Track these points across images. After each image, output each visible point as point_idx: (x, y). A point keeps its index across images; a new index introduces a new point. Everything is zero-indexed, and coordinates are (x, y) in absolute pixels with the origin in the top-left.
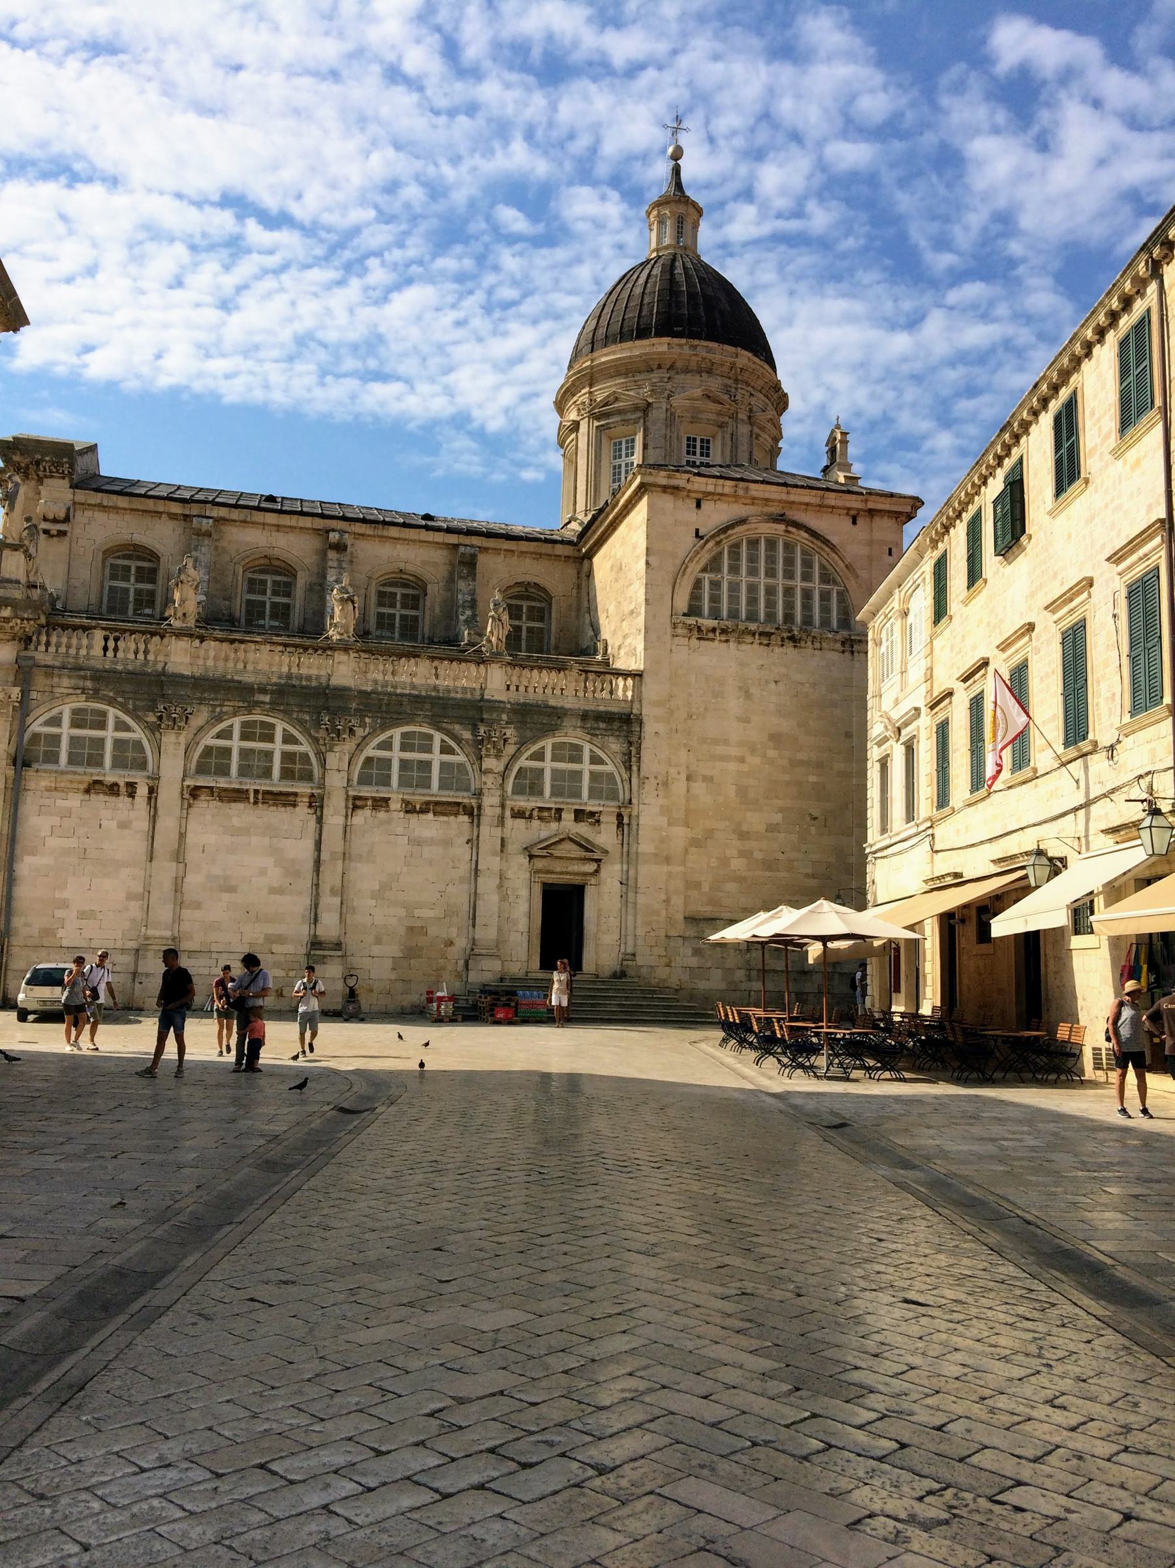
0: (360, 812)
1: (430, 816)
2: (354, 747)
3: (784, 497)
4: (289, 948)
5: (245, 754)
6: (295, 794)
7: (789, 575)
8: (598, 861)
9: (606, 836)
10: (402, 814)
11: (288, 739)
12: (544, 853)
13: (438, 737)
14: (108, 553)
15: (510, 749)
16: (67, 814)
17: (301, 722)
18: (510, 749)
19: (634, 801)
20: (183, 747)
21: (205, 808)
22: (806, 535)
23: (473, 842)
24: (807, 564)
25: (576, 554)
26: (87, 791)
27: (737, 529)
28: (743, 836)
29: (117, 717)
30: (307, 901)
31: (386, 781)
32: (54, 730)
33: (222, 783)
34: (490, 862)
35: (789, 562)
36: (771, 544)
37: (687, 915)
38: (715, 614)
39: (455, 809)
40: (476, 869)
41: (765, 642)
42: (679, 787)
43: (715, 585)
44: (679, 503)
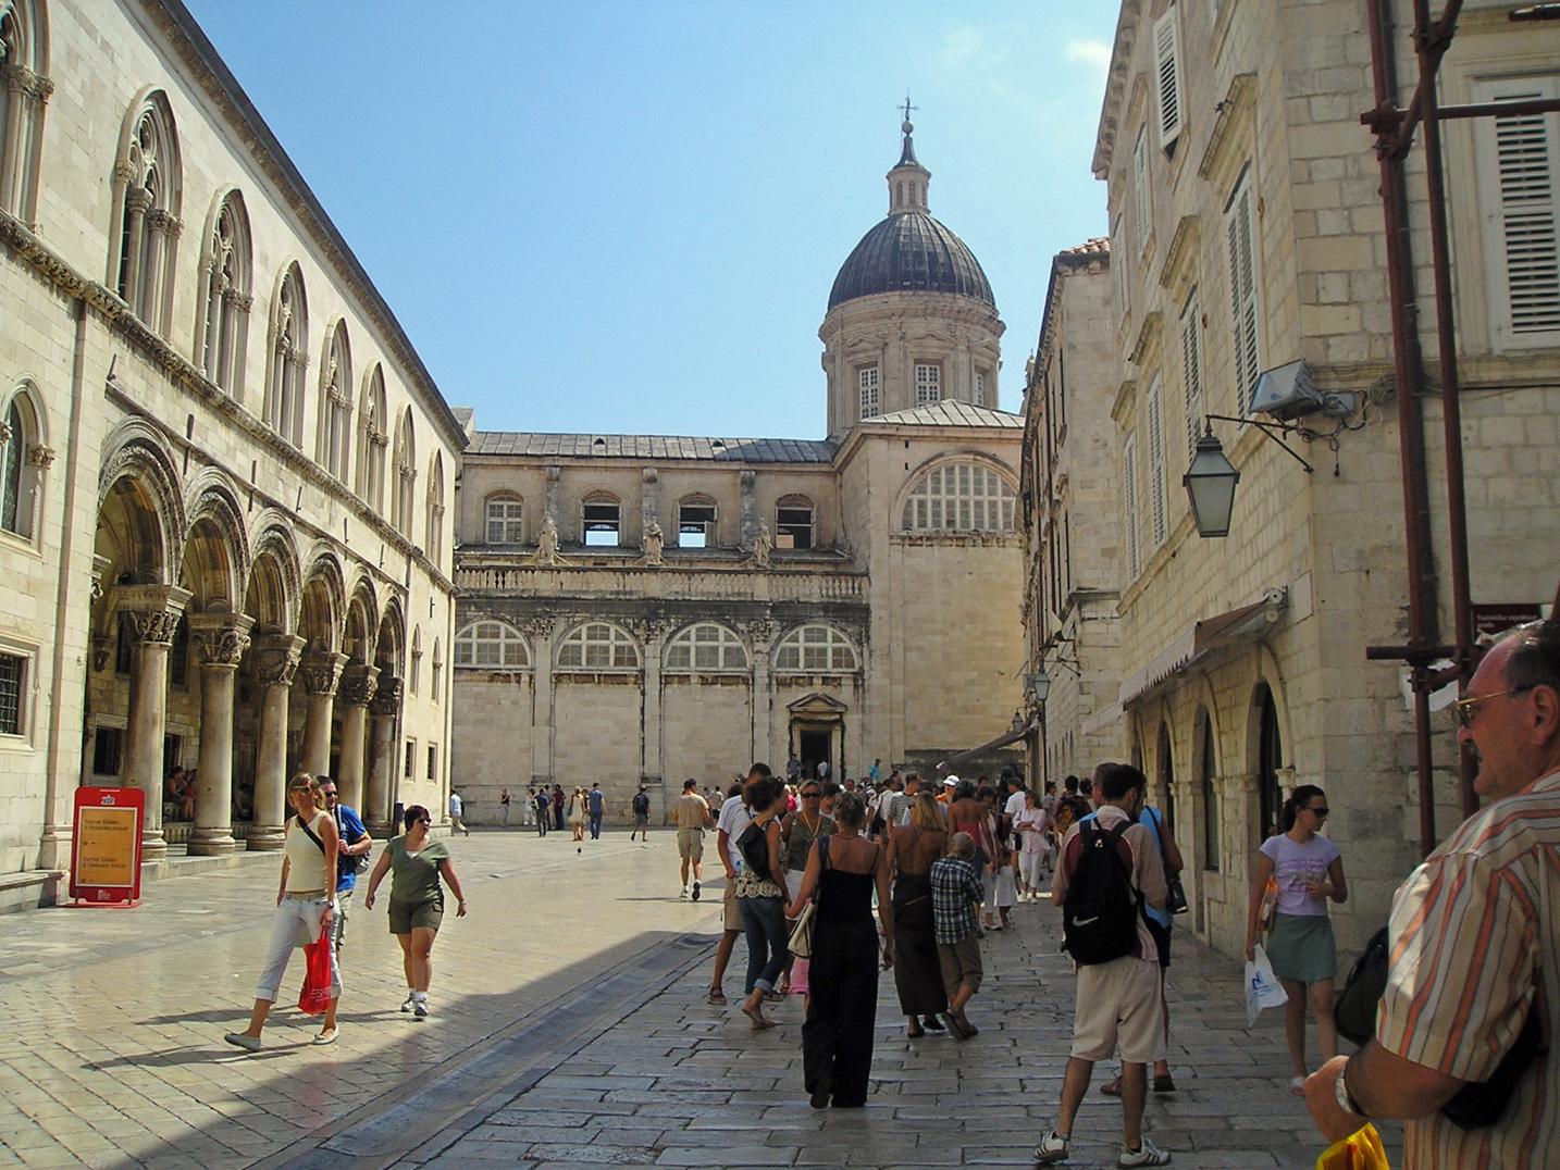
0: (668, 686)
1: (719, 686)
2: (664, 640)
3: (970, 435)
4: (627, 783)
5: (591, 649)
6: (625, 675)
7: (978, 492)
8: (841, 713)
9: (845, 694)
10: (699, 686)
11: (619, 636)
12: (800, 709)
13: (722, 629)
14: (487, 498)
15: (775, 636)
16: (477, 696)
17: (626, 625)
18: (775, 636)
19: (866, 668)
20: (550, 647)
21: (567, 689)
22: (990, 461)
23: (750, 703)
24: (992, 482)
25: (832, 469)
26: (491, 681)
27: (937, 461)
28: (948, 690)
29: (506, 629)
30: (638, 748)
31: (685, 662)
32: (467, 640)
33: (576, 670)
34: (762, 718)
35: (978, 482)
36: (964, 470)
37: (907, 748)
38: (922, 524)
39: (735, 680)
40: (753, 723)
41: (961, 544)
42: (898, 656)
43: (922, 504)
44: (892, 445)
